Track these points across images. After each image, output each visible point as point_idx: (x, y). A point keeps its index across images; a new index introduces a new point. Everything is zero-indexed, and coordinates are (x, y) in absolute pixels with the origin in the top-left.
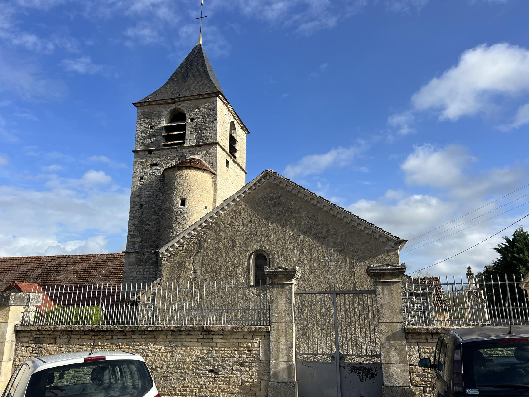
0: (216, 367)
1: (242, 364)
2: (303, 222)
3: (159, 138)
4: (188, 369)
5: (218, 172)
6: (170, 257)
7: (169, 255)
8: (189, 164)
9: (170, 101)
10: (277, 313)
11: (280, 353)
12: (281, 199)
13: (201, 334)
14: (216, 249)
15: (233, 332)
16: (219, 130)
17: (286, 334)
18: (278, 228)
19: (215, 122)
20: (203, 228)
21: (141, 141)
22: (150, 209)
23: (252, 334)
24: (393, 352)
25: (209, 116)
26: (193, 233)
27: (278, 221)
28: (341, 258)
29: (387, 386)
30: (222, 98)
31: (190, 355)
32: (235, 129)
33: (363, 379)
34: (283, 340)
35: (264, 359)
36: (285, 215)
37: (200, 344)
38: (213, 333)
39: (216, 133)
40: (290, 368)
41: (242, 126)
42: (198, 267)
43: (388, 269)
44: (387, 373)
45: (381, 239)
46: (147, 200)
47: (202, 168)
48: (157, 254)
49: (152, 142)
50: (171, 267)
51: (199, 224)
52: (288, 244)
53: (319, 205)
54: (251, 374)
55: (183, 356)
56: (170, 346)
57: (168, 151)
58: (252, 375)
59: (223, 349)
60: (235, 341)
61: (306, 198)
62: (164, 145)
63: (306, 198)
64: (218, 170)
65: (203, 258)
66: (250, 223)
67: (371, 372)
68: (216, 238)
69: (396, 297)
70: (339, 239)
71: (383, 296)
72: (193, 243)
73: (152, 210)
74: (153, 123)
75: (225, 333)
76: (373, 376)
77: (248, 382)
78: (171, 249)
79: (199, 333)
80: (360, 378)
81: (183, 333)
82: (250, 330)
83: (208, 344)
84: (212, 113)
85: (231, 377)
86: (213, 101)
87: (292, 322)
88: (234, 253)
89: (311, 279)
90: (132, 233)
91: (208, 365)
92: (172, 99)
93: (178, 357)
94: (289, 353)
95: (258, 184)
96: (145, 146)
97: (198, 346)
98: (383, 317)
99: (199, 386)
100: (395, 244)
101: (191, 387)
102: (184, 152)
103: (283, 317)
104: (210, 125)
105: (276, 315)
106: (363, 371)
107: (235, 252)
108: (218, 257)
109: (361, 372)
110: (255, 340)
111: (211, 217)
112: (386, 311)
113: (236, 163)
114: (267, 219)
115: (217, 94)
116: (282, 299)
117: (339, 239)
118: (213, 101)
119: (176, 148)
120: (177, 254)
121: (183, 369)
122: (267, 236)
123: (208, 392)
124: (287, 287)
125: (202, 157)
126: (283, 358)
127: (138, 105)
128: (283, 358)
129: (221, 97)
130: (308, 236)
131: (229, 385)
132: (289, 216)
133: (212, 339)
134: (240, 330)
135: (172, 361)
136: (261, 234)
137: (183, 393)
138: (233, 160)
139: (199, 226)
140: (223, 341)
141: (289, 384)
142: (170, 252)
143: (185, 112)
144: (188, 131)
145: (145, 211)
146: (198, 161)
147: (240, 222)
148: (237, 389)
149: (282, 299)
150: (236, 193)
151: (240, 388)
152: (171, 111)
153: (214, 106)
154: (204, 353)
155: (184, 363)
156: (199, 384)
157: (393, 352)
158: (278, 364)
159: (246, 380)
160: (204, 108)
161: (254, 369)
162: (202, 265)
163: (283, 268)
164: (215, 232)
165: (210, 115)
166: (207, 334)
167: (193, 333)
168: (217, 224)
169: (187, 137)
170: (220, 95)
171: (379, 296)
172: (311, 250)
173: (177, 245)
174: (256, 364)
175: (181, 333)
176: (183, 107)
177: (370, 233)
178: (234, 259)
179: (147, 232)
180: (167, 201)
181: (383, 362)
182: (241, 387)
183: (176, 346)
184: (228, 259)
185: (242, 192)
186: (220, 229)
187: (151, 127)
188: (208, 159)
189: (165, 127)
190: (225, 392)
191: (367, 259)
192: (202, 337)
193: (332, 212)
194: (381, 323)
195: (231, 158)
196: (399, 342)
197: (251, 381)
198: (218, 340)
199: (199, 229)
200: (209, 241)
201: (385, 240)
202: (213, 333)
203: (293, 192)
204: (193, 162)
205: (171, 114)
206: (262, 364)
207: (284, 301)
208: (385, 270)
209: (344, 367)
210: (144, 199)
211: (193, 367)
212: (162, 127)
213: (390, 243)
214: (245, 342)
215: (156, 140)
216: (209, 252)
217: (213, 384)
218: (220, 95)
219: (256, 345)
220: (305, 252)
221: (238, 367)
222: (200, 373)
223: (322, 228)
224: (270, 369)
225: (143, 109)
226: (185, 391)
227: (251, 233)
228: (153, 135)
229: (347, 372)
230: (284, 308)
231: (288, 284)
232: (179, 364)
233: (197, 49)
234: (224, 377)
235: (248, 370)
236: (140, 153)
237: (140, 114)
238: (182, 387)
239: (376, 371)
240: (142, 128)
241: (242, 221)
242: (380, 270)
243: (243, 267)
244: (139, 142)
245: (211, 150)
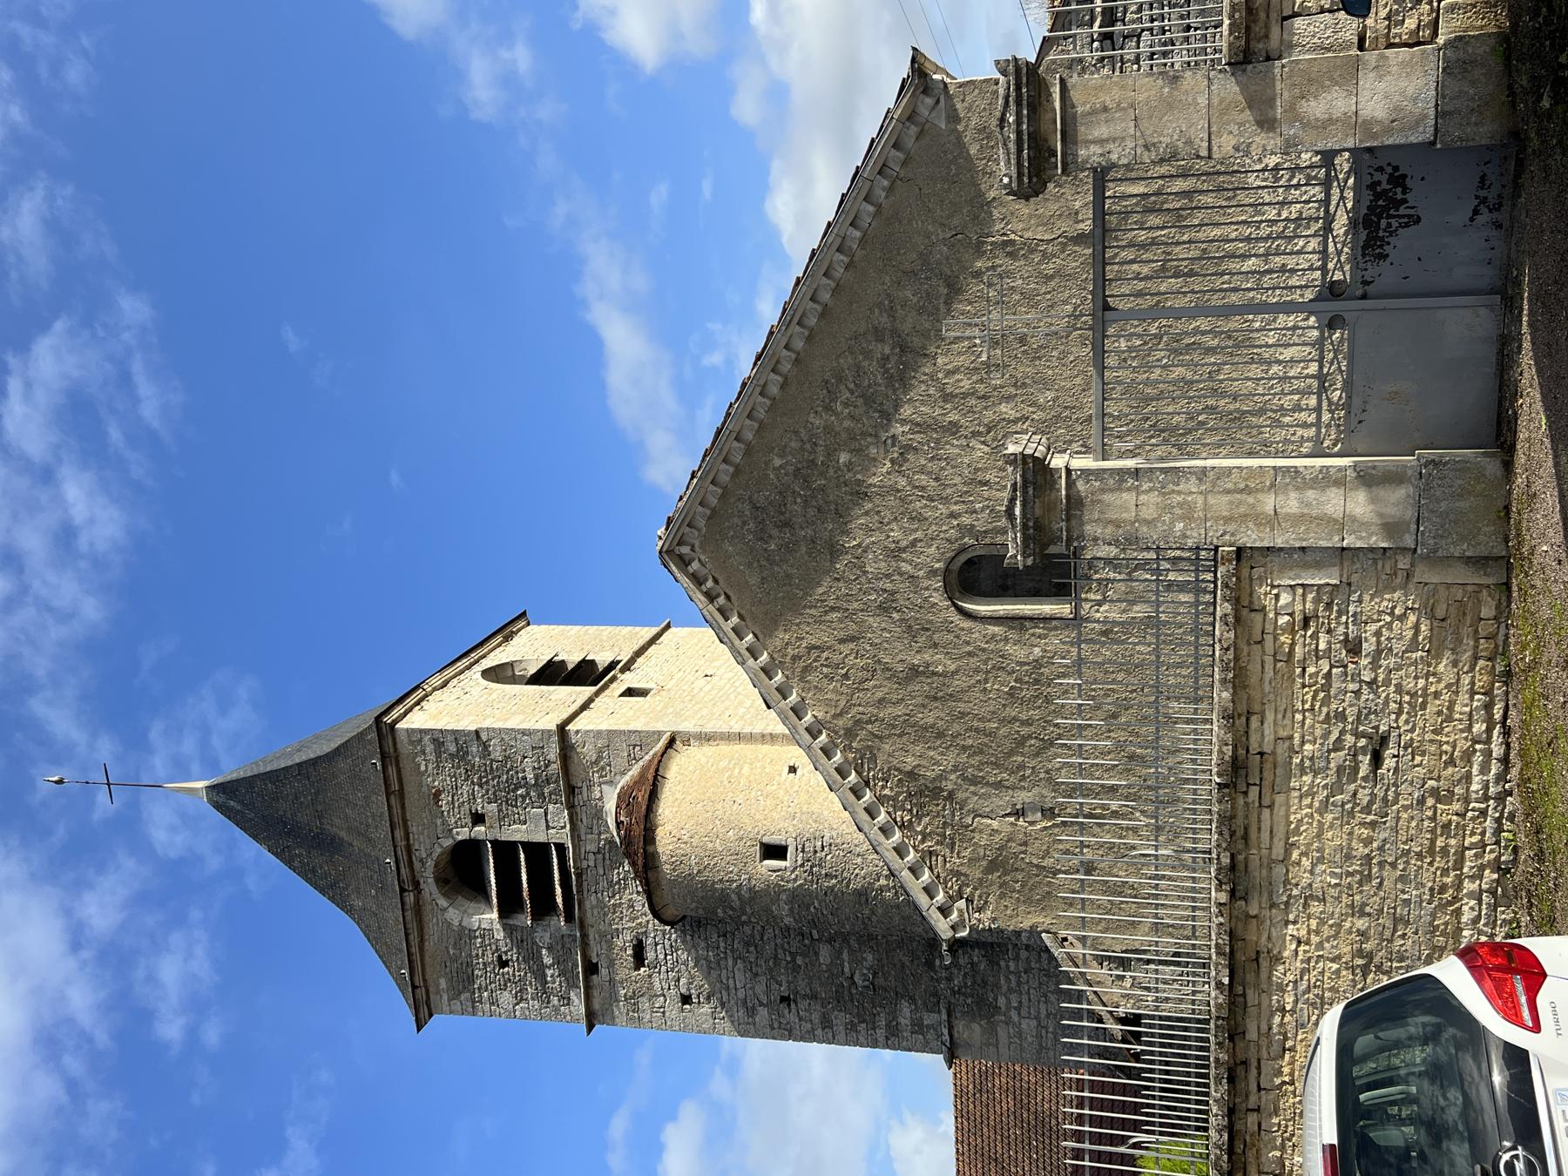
0: (1362, 742)
1: (1354, 647)
2: (847, 423)
3: (543, 937)
4: (1368, 842)
5: (666, 726)
6: (969, 901)
7: (962, 904)
8: (638, 831)
9: (410, 898)
10: (1172, 523)
11: (1314, 513)
12: (762, 502)
13: (1246, 793)
14: (941, 735)
15: (1238, 680)
16: (513, 723)
17: (1247, 490)
18: (867, 513)
19: (484, 737)
20: (867, 784)
21: (555, 1000)
22: (796, 969)
23: (1245, 612)
24: (1315, 108)
25: (463, 758)
26: (882, 817)
27: (841, 516)
28: (975, 288)
29: (1436, 129)
30: (400, 710)
31: (1319, 836)
32: (511, 664)
33: (1409, 216)
34: (1268, 503)
35: (1336, 571)
36: (822, 489)
37: (1280, 799)
38: (1242, 752)
39: (524, 732)
40: (1367, 479)
41: (499, 638)
42: (1003, 801)
43: (1019, 122)
44: (1388, 131)
45: (910, 143)
46: (763, 979)
47: (652, 783)
48: (956, 945)
49: (557, 962)
50: (1002, 896)
51: (852, 797)
52: (923, 479)
53: (786, 367)
54: (1390, 617)
55: (1321, 860)
56: (1287, 903)
57: (588, 905)
58: (1392, 614)
59: (1299, 717)
60: (1269, 673)
61: (761, 413)
62: (569, 918)
63: (761, 413)
64: (659, 727)
65: (974, 781)
66: (849, 615)
67: (1386, 187)
68: (900, 736)
69: (1116, 93)
70: (909, 294)
71: (1114, 140)
72: (919, 817)
73: (799, 961)
74: (489, 957)
75: (1242, 708)
76: (1399, 180)
77: (1416, 627)
78: (940, 897)
79: (1241, 801)
80: (1407, 225)
81: (1241, 857)
82: (1231, 619)
83: (1279, 771)
84: (452, 748)
85: (1399, 689)
86: (411, 742)
87: (1204, 470)
88: (956, 672)
89: (1050, 395)
90: (881, 1033)
91: (1356, 770)
92: (402, 890)
93: (1326, 877)
94: (1315, 480)
95: (710, 584)
96: (572, 985)
97: (1289, 807)
98: (1189, 142)
99: (1430, 802)
100: (925, 92)
101: (1433, 831)
102: (591, 847)
103: (1185, 502)
104: (497, 754)
105: (1180, 526)
106: (1380, 217)
107: (953, 667)
108: (970, 729)
109: (1383, 223)
110: (1268, 602)
111: (827, 752)
112: (1169, 132)
113: (632, 661)
114: (835, 551)
115: (383, 730)
116: (1123, 504)
117: (909, 294)
118: (411, 742)
119: (579, 876)
120: (958, 874)
121: (1369, 858)
122: (895, 553)
123: (1450, 770)
124: (1081, 486)
125: (611, 783)
126: (1333, 502)
127: (423, 1012)
128: (1333, 502)
129: (395, 714)
130: (897, 406)
131: (1425, 695)
132: (823, 474)
133: (1261, 754)
134: (1230, 655)
135: (1338, 899)
136: (887, 576)
137: (1452, 858)
138: (622, 671)
139: (859, 798)
140: (1270, 717)
141: (1426, 481)
142: (952, 899)
143: (448, 843)
144: (517, 833)
145: (802, 986)
146: (625, 799)
147: (846, 648)
148: (1441, 668)
149: (1123, 504)
150: (742, 663)
151: (1439, 657)
152: (445, 895)
154: (1312, 785)
155: (1348, 857)
156: (1421, 801)
157: (1315, 108)
158: (1354, 519)
159: (1409, 634)
160: (434, 775)
161: (1369, 606)
162: (999, 785)
163: (1012, 500)
164: (880, 738)
165: (461, 755)
166: (1243, 772)
167: (1240, 821)
168: (850, 733)
169: (540, 837)
170: (388, 719)
171: (1114, 157)
172: (947, 397)
173: (926, 876)
174: (1355, 597)
175: (1241, 867)
176: (430, 851)
177: (886, 183)
178: (977, 671)
179: (880, 981)
180: (768, 910)
181: (1350, 144)
182: (1434, 653)
183: (1286, 882)
184: (976, 694)
185: (737, 642)
186: (869, 722)
187: (503, 964)
188: (619, 762)
189: (504, 913)
190: (1451, 708)
191: (981, 194)
192: (1254, 792)
193: (812, 321)
194: (1210, 149)
195: (614, 679)
196: (1278, 86)
197: (1412, 618)
198: (1265, 734)
199: (868, 796)
200: (910, 762)
201: (914, 130)
202: (1242, 752)
203: (737, 458)
204: (629, 814)
205: (458, 892)
206: (1355, 578)
207: (1128, 497)
208: (1019, 133)
209: (1366, 283)
210: (760, 989)
211: (1363, 824)
212: (505, 927)
213: (924, 112)
214: (1275, 639)
215: (549, 949)
216: (950, 759)
217: (1423, 754)
218: (388, 719)
219: (1285, 599)
220: (953, 417)
221: (1364, 662)
222: (1385, 799)
223: (867, 354)
224: (1371, 550)
225: (438, 992)
226: (1445, 851)
227: (884, 609)
228: (531, 957)
229: (1385, 275)
230: (1154, 498)
231: (1070, 484)
232: (1349, 874)
233: (221, 798)
234: (1399, 713)
235: (1373, 627)
236: (596, 1005)
237: (456, 1005)
238: (1431, 864)
239: (1381, 169)
240: (506, 998)
241: (842, 641)
242: (1020, 151)
243: (1006, 640)
244: (557, 1010)
245: (587, 752)
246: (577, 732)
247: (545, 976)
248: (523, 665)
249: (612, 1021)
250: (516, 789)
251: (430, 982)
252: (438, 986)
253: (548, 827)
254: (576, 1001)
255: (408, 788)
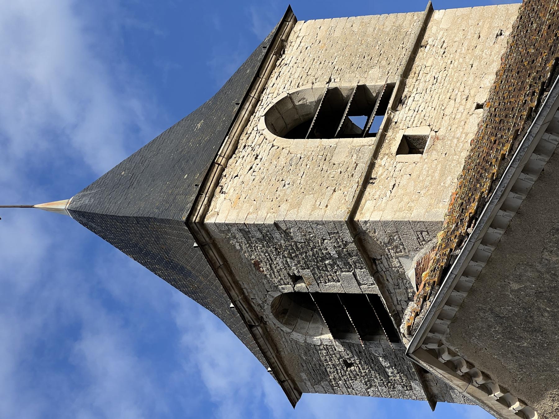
9: (259, 331)
19: (283, 227)
30: (204, 200)
41: (272, 57)
118: (221, 232)
127: (293, 394)
129: (200, 209)
152: (286, 324)
153: (234, 229)
170: (196, 218)
187: (350, 365)
188: (411, 240)
215: (385, 357)
218: (196, 218)
228: (372, 362)
240: (358, 384)
245: (380, 236)
246: (366, 222)
247: (387, 373)
248: (300, 96)
249: (452, 400)
250: (323, 260)
251: (293, 375)
252: (301, 377)
253: (359, 284)
254: (418, 388)
255: (232, 260)
